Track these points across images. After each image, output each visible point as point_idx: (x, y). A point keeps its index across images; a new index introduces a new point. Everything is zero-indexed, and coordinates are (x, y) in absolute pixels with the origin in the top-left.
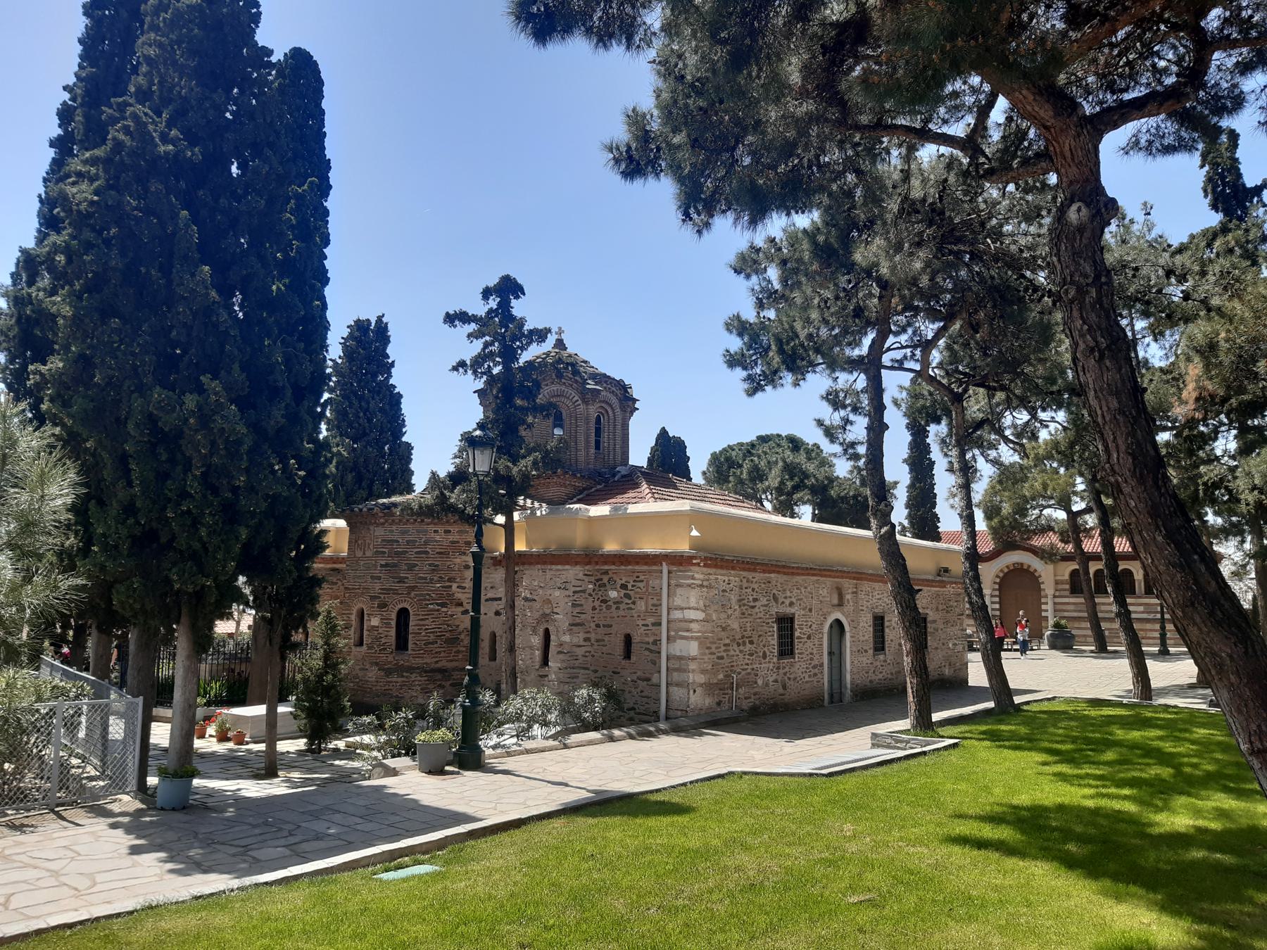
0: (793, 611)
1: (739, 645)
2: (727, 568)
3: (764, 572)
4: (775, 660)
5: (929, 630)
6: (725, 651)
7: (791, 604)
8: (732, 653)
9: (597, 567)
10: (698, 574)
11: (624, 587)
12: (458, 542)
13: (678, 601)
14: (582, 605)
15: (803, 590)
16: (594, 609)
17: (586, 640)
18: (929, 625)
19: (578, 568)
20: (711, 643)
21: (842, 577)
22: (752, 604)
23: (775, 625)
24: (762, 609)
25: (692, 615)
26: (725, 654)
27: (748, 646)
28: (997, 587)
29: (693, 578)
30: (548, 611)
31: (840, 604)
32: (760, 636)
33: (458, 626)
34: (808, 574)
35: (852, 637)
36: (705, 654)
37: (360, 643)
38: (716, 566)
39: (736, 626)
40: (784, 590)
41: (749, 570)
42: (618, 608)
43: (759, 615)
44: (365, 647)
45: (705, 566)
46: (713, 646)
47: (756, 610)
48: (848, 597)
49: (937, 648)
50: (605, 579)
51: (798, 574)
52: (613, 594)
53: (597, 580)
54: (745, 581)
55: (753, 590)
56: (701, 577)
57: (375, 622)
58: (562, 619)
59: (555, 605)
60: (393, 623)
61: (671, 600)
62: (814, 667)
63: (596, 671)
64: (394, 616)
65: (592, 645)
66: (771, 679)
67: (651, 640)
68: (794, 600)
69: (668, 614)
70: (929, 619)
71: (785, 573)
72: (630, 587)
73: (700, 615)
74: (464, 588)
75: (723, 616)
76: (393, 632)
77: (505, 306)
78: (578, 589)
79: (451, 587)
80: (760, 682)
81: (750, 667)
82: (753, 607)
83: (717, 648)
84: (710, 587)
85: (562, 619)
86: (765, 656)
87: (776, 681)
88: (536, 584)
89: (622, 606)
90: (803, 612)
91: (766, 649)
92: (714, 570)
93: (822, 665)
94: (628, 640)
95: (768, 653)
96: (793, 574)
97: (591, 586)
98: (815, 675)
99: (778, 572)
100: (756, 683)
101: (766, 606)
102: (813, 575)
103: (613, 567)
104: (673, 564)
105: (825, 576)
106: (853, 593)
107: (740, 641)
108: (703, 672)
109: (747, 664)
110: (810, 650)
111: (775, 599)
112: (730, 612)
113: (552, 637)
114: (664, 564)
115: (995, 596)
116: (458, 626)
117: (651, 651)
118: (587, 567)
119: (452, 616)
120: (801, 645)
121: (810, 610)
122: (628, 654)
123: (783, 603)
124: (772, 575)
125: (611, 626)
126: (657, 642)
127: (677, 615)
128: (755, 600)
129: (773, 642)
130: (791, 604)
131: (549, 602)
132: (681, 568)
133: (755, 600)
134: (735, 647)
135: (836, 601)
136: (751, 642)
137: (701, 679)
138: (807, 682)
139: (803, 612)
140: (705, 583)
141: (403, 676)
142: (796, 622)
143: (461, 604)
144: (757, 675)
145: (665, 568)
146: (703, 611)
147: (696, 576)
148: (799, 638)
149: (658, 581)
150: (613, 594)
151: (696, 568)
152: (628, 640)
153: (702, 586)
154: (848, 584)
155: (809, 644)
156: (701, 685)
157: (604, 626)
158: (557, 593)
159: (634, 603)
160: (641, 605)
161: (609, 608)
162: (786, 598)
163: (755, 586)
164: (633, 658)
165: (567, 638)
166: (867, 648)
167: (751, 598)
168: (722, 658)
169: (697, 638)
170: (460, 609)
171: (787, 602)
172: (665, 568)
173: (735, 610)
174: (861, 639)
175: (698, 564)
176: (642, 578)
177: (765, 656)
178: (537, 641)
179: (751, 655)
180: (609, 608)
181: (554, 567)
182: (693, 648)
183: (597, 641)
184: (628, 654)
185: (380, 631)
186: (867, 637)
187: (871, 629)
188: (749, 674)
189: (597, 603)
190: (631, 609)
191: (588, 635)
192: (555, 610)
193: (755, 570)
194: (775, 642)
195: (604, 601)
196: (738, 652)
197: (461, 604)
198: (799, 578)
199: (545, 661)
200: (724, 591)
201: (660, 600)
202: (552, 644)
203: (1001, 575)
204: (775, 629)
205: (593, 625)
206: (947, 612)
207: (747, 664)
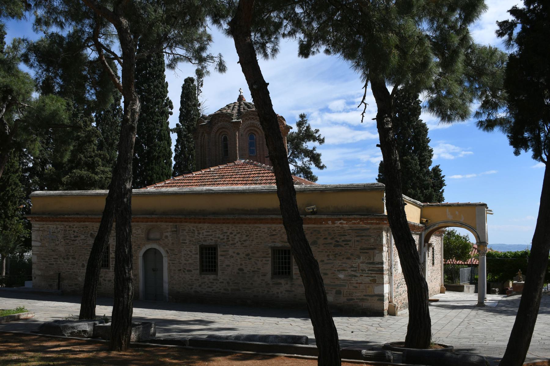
1: (64, 259)
6: (54, 261)
8: (59, 262)
22: (73, 239)
24: (81, 241)
26: (54, 263)
27: (71, 260)
32: (80, 255)
47: (77, 242)
54: (67, 227)
55: (74, 231)
112: (57, 243)
124: (87, 223)
136: (74, 258)
140: (41, 229)
146: (40, 242)
153: (37, 230)
163: (76, 230)
167: (72, 236)
168: (53, 264)
179: (74, 265)
196: (63, 263)
207: (70, 269)
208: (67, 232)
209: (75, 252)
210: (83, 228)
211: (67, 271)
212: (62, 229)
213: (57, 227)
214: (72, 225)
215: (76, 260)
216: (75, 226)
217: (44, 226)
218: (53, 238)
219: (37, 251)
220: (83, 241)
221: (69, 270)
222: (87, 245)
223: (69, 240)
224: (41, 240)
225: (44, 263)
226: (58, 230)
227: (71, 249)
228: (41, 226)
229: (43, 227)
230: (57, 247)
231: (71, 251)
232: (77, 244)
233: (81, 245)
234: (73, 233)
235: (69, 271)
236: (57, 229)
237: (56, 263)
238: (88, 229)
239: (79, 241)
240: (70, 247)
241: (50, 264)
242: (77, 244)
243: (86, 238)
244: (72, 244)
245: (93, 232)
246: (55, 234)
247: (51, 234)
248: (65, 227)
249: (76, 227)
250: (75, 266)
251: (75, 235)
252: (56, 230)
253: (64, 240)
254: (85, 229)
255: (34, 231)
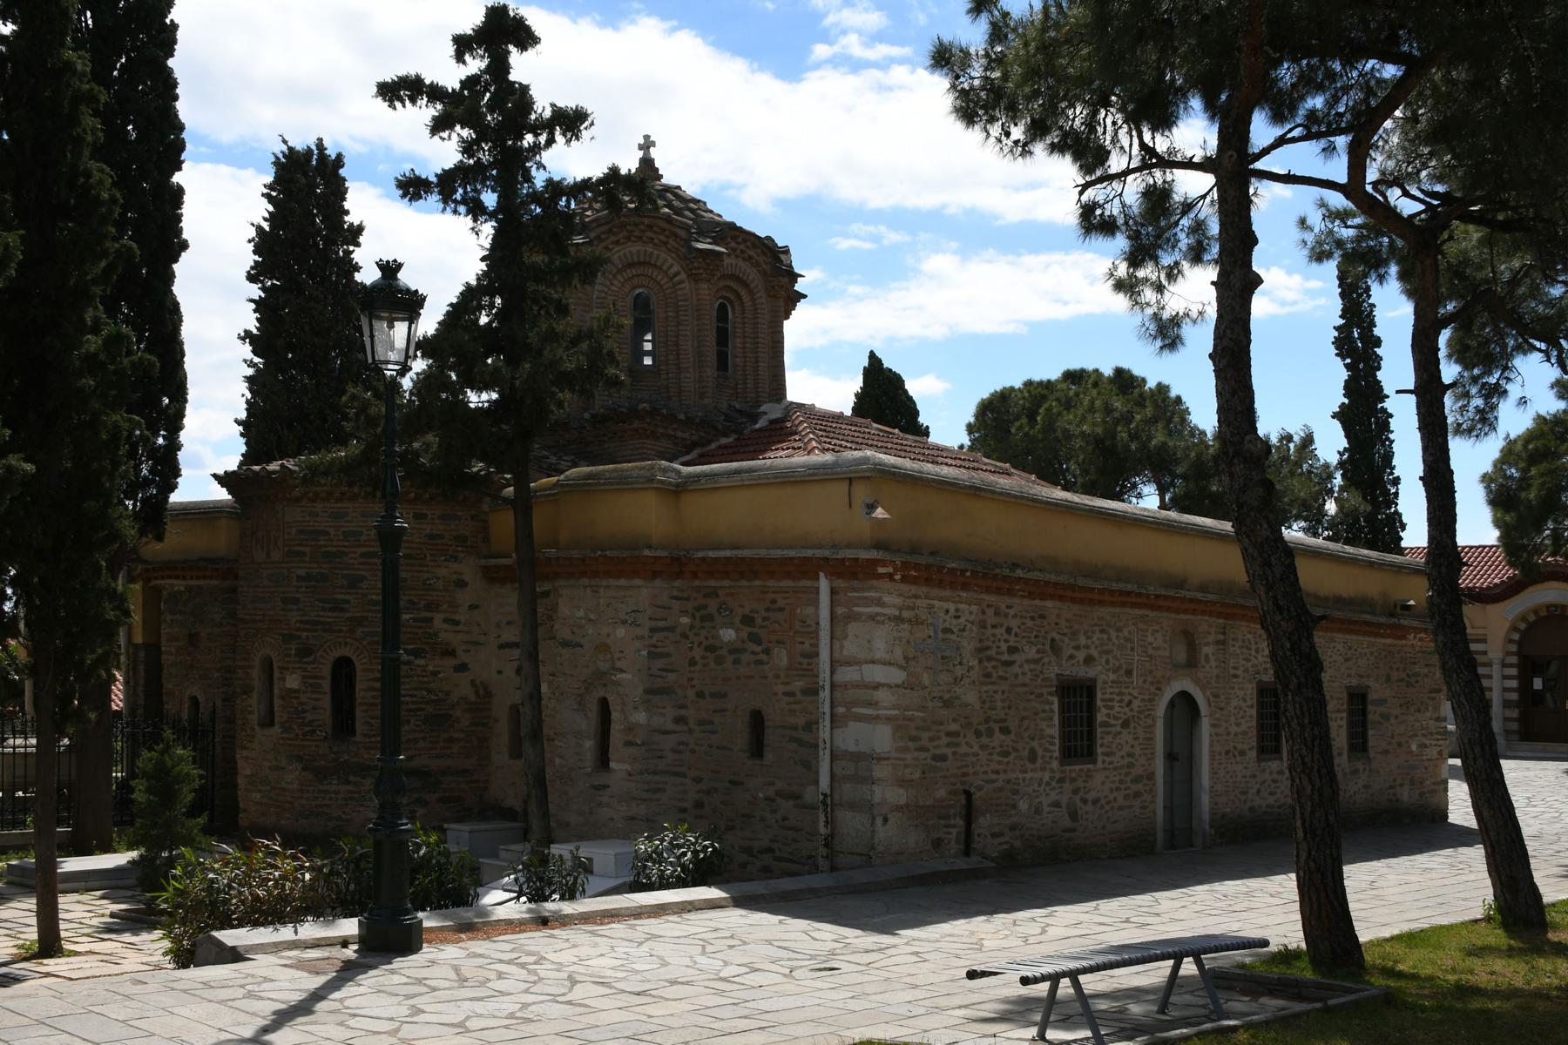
0: (1091, 672)
1: (978, 734)
2: (952, 586)
3: (1031, 596)
4: (1055, 764)
5: (1370, 717)
6: (948, 745)
7: (1089, 660)
8: (964, 749)
9: (697, 583)
10: (891, 598)
11: (748, 620)
12: (442, 537)
13: (850, 648)
14: (668, 655)
15: (1113, 634)
16: (693, 662)
17: (680, 720)
18: (1370, 708)
19: (658, 582)
20: (918, 728)
21: (1194, 612)
22: (1006, 657)
23: (1055, 700)
24: (1026, 667)
25: (877, 674)
26: (948, 752)
27: (999, 738)
28: (1514, 648)
29: (879, 602)
30: (604, 666)
31: (1192, 663)
32: (1023, 719)
33: (448, 693)
34: (1123, 604)
35: (1213, 726)
36: (907, 749)
37: (268, 721)
38: (928, 581)
39: (971, 697)
40: (1075, 634)
41: (999, 591)
42: (737, 662)
43: (1021, 679)
44: (277, 729)
45: (904, 579)
46: (925, 735)
47: (1015, 669)
48: (1208, 650)
49: (1386, 752)
50: (712, 605)
51: (1101, 603)
52: (728, 635)
53: (698, 608)
54: (990, 612)
55: (1009, 630)
56: (898, 601)
57: (293, 682)
58: (630, 680)
59: (617, 655)
60: (326, 685)
61: (837, 645)
62: (1137, 780)
63: (698, 780)
64: (326, 671)
65: (691, 731)
66: (1046, 801)
67: (800, 721)
68: (1095, 653)
69: (832, 673)
70: (1372, 696)
71: (1074, 600)
72: (759, 621)
73: (897, 676)
74: (457, 623)
75: (944, 678)
76: (326, 702)
77: (499, 67)
78: (661, 624)
79: (430, 620)
80: (1023, 805)
81: (1002, 777)
82: (1009, 664)
83: (931, 739)
84: (916, 622)
85: (630, 680)
86: (1033, 757)
87: (1057, 804)
88: (581, 614)
89: (746, 658)
90: (1112, 677)
91: (1035, 744)
92: (925, 589)
93: (1151, 776)
94: (757, 721)
95: (1040, 752)
96: (1091, 602)
97: (685, 620)
98: (1137, 795)
99: (1061, 598)
100: (1014, 806)
101: (1036, 661)
102: (1133, 605)
103: (726, 583)
104: (839, 575)
105: (1160, 608)
106: (1218, 643)
107: (982, 728)
108: (903, 783)
109: (997, 772)
110: (1127, 749)
111: (1055, 648)
112: (959, 671)
113: (615, 715)
114: (822, 574)
115: (1511, 665)
116: (448, 693)
117: (800, 742)
118: (677, 583)
119: (435, 674)
120: (1109, 738)
121: (1129, 673)
122: (757, 749)
123: (1071, 657)
124: (1049, 604)
125: (723, 695)
126: (811, 726)
127: (847, 674)
128: (1013, 650)
129: (1049, 731)
130: (1089, 660)
131: (603, 648)
132: (855, 583)
133: (1013, 650)
134: (971, 737)
135: (1181, 655)
136: (1005, 731)
137: (897, 796)
138: (1121, 808)
139: (1112, 677)
140: (906, 614)
141: (348, 782)
142: (1099, 695)
143: (451, 653)
144: (1016, 792)
145: (824, 584)
146: (901, 667)
147: (887, 599)
148: (1104, 724)
149: (811, 610)
150: (728, 635)
151: (887, 584)
152: (757, 721)
153: (898, 619)
154: (1207, 628)
155: (1126, 736)
156: (899, 808)
157: (713, 695)
158: (621, 632)
159: (767, 652)
160: (781, 657)
161: (719, 660)
162: (1077, 648)
163: (1014, 624)
164: (769, 757)
165: (641, 717)
166: (1245, 747)
167: (1004, 647)
168: (943, 758)
169: (889, 719)
170: (452, 662)
171: (1081, 656)
172: (824, 584)
173: (970, 669)
174: (1234, 729)
175: (890, 576)
176: (781, 603)
177: (1033, 757)
178: (586, 723)
179: (1006, 754)
180: (719, 660)
181: (612, 582)
182: (881, 738)
183: (701, 723)
184: (757, 749)
185: (303, 698)
186: (1244, 727)
187: (1254, 712)
188: (1001, 790)
189: (697, 653)
190: (761, 663)
191: (683, 712)
192: (619, 664)
193: (1010, 592)
194: (1055, 731)
195: (711, 649)
196: (976, 748)
197: (451, 653)
198: (1105, 612)
199: (603, 761)
200: (946, 631)
201: (816, 645)
202: (616, 727)
203: (1523, 626)
204: (1056, 707)
205: (691, 694)
206: (1409, 685)
207: (997, 772)
208: (989, 631)
209: (1009, 708)
210: (1032, 618)
211: (988, 782)
212: (972, 618)
213: (957, 610)
214: (1003, 606)
215: (1012, 736)
216: (1012, 612)
217: (918, 602)
218: (948, 653)
219: (894, 707)
220: (1032, 666)
221: (994, 777)
222: (1044, 680)
223: (994, 663)
224: (906, 658)
225: (916, 754)
226: (962, 620)
227: (998, 696)
228: (909, 602)
229: (913, 608)
230: (958, 690)
231: (999, 704)
232: (1016, 676)
233: (1027, 679)
234: (1006, 636)
235: (993, 781)
236: (958, 617)
237: (954, 753)
238: (1045, 623)
239: (1021, 666)
240: (995, 687)
241: (936, 758)
242: (1016, 676)
243: (1040, 655)
244: (1001, 678)
245: (1057, 637)
246: (953, 637)
247: (940, 635)
248: (983, 613)
249: (1015, 616)
250: (1011, 758)
251: (1011, 644)
252: (955, 622)
253: (980, 661)
254: (1038, 622)
255: (883, 623)
